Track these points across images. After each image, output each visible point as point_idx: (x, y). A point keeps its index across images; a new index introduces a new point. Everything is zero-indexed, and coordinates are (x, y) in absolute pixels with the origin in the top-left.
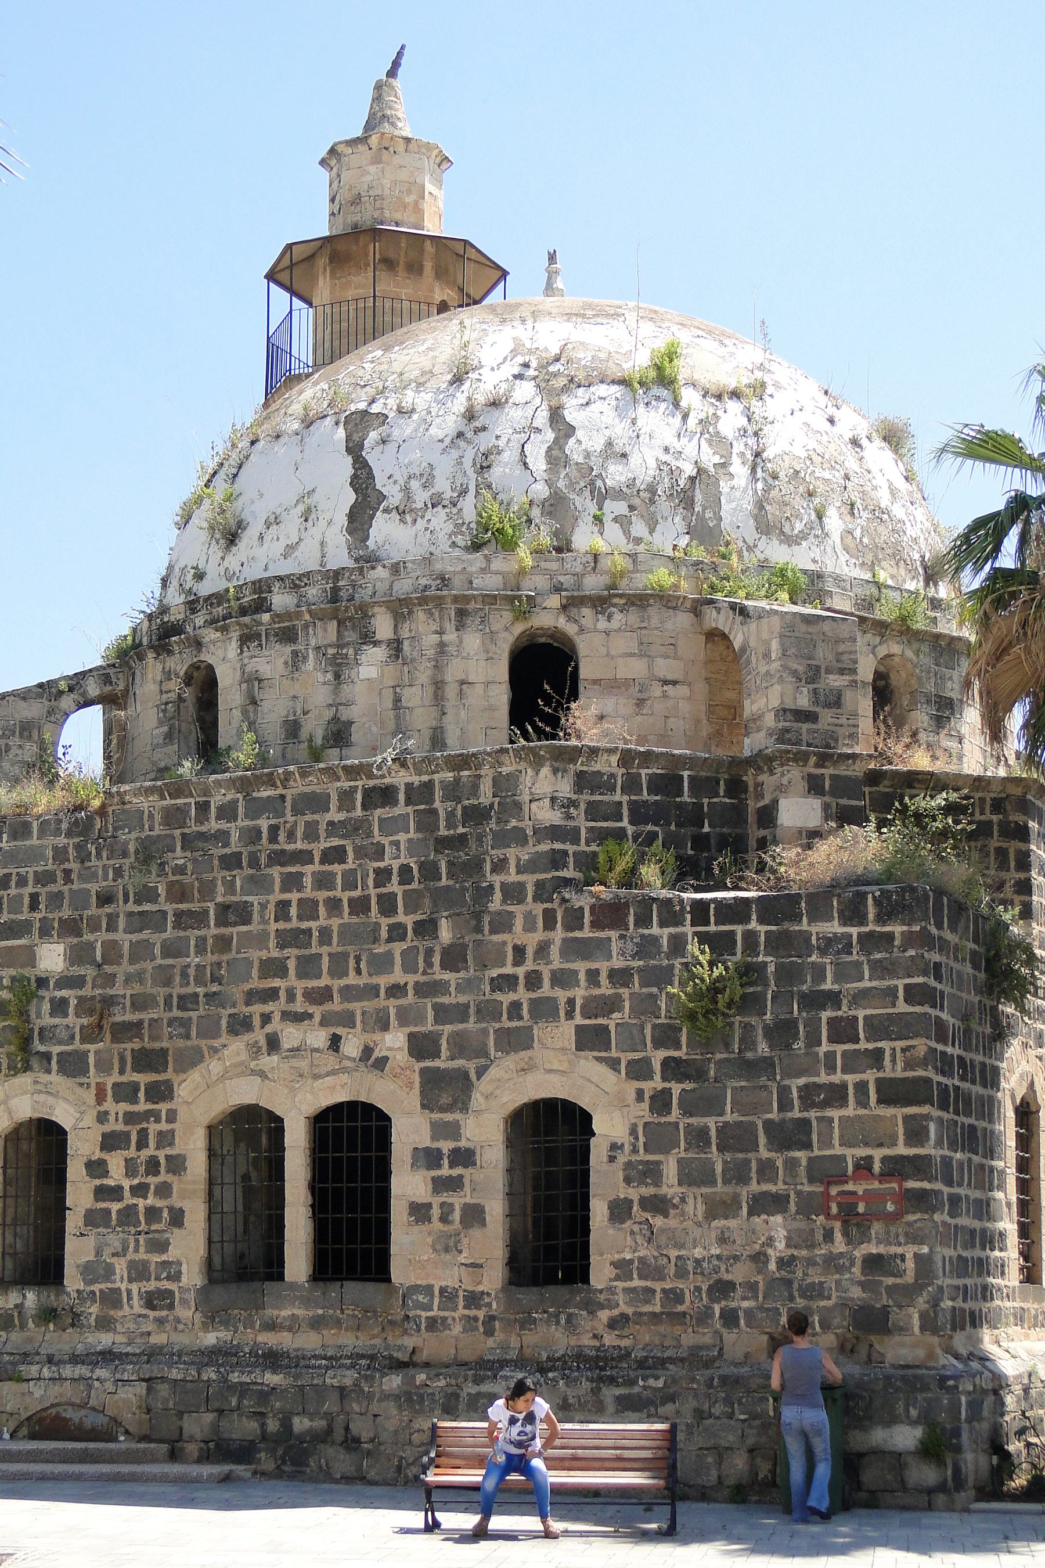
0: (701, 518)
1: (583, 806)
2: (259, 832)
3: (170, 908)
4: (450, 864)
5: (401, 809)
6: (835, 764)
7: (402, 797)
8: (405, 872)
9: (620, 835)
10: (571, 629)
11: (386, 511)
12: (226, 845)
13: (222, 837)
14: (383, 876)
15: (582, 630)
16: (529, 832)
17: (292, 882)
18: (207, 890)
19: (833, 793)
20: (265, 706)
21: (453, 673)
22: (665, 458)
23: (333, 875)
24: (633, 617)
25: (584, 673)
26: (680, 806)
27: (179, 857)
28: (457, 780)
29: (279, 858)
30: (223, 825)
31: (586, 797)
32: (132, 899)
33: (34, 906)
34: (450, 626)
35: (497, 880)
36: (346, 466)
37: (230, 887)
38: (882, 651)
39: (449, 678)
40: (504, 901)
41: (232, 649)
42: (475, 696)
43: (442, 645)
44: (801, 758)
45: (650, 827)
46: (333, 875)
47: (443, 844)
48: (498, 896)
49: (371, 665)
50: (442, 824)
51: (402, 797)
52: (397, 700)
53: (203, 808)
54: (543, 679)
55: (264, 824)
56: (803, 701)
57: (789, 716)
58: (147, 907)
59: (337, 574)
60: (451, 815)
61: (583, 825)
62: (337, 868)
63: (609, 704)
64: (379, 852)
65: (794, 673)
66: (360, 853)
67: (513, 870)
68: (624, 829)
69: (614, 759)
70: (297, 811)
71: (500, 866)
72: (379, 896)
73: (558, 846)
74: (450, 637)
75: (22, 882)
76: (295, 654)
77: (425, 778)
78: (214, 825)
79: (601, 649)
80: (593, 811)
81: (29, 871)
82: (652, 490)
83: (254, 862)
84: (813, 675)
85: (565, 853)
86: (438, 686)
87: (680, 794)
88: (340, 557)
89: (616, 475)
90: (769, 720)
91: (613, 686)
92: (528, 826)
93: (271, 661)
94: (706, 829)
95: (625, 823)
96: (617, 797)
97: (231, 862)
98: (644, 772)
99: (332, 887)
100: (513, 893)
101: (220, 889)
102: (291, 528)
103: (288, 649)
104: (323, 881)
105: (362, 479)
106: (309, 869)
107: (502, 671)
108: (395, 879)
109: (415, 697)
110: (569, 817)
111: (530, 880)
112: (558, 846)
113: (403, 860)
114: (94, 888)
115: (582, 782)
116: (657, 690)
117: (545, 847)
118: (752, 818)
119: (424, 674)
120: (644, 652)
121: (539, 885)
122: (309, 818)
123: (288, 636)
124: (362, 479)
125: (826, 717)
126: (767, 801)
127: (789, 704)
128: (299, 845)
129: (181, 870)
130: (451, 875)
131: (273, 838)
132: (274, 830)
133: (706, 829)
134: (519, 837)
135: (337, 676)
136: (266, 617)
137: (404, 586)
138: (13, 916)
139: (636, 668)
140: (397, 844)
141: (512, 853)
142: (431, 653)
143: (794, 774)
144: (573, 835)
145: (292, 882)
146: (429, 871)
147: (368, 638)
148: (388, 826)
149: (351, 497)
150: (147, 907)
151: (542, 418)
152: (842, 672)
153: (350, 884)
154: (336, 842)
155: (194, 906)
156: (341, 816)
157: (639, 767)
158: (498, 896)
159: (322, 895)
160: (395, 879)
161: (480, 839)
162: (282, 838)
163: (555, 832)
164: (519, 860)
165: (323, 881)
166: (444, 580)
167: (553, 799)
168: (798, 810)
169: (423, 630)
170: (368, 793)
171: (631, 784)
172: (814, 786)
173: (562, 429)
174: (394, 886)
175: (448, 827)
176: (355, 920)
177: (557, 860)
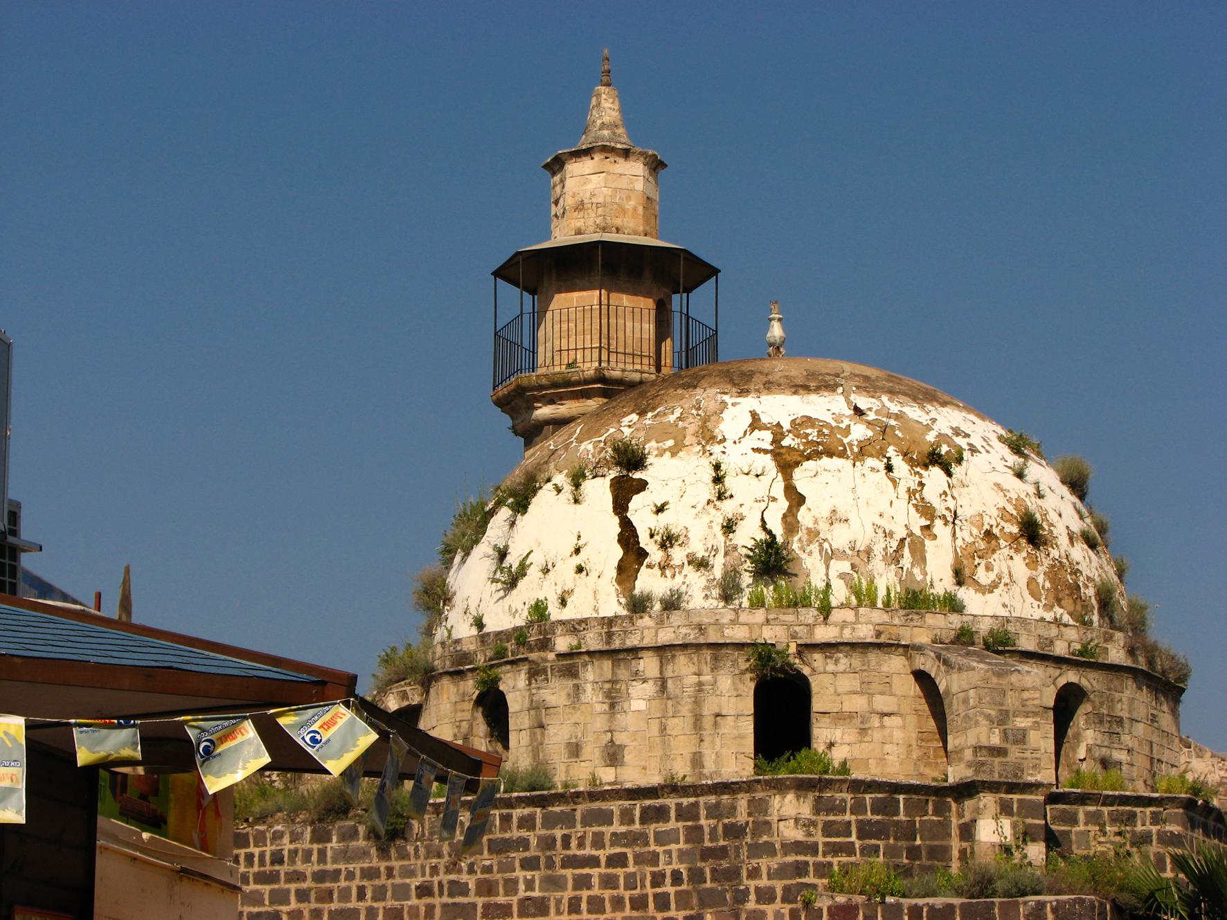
0: (910, 573)
1: (820, 826)
2: (554, 840)
3: (480, 901)
4: (713, 871)
5: (672, 824)
6: (1022, 792)
7: (673, 814)
8: (677, 878)
9: (849, 849)
10: (806, 671)
11: (650, 566)
12: (527, 848)
13: (524, 844)
14: (658, 880)
15: (813, 670)
16: (778, 846)
17: (583, 882)
18: (511, 886)
19: (1019, 814)
20: (551, 730)
21: (708, 709)
22: (879, 521)
23: (617, 877)
24: (856, 660)
25: (817, 705)
26: (897, 823)
27: (486, 859)
28: (718, 804)
29: (571, 862)
30: (524, 833)
31: (823, 818)
32: (446, 893)
33: (361, 895)
34: (706, 669)
35: (752, 884)
36: (613, 526)
37: (530, 885)
38: (1062, 682)
39: (705, 712)
40: (758, 902)
41: (522, 680)
42: (727, 726)
43: (700, 684)
44: (993, 787)
45: (873, 842)
46: (617, 877)
47: (707, 854)
48: (752, 897)
49: (640, 697)
50: (707, 837)
51: (673, 814)
52: (663, 729)
53: (506, 819)
54: (783, 712)
55: (558, 833)
56: (996, 740)
57: (984, 752)
58: (460, 900)
59: (610, 622)
60: (713, 831)
61: (820, 839)
62: (619, 871)
63: (837, 734)
64: (654, 859)
65: (988, 717)
66: (639, 859)
67: (765, 876)
68: (853, 843)
69: (845, 787)
70: (585, 823)
71: (754, 873)
72: (656, 896)
73: (801, 858)
74: (706, 678)
75: (350, 876)
76: (577, 687)
77: (692, 800)
78: (515, 833)
79: (830, 687)
80: (829, 829)
81: (356, 867)
82: (869, 551)
83: (550, 864)
84: (1003, 718)
85: (807, 863)
86: (698, 720)
87: (897, 813)
88: (612, 606)
89: (839, 538)
90: (968, 754)
91: (841, 717)
92: (776, 840)
93: (555, 692)
94: (918, 842)
95: (853, 838)
96: (847, 817)
97: (529, 864)
98: (867, 796)
99: (616, 887)
100: (766, 896)
101: (522, 886)
102: (564, 574)
103: (570, 683)
104: (609, 882)
105: (628, 536)
106: (595, 872)
107: (748, 705)
108: (668, 880)
109: (679, 725)
110: (809, 834)
111: (779, 885)
112: (801, 858)
113: (675, 866)
114: (415, 882)
115: (818, 808)
116: (875, 721)
117: (790, 859)
118: (955, 831)
119: (686, 709)
120: (865, 690)
121: (786, 889)
122: (596, 829)
123: (571, 672)
124: (628, 536)
125: (1014, 753)
126: (967, 818)
127: (984, 742)
128: (588, 851)
129: (488, 869)
130: (713, 880)
131: (566, 845)
132: (566, 840)
133: (918, 842)
134: (769, 850)
135: (612, 706)
136: (551, 656)
137: (666, 636)
138: (343, 905)
139: (858, 704)
140: (669, 853)
141: (764, 863)
142: (690, 691)
143: (988, 800)
144: (812, 849)
145: (583, 882)
146: (696, 876)
147: (636, 676)
148: (661, 838)
149: (619, 552)
150: (460, 900)
151: (779, 489)
152: (1027, 715)
153: (630, 885)
154: (618, 850)
155: (501, 899)
156: (623, 829)
157: (864, 792)
158: (752, 897)
159: (607, 894)
160: (668, 880)
161: (737, 849)
162: (574, 843)
163: (798, 847)
164: (769, 869)
165: (609, 882)
166: (701, 628)
167: (797, 820)
168: (992, 830)
169: (684, 668)
170: (645, 811)
171: (858, 808)
172: (1005, 809)
173: (796, 499)
174: (669, 889)
175: (711, 840)
176: (635, 914)
177: (800, 869)
